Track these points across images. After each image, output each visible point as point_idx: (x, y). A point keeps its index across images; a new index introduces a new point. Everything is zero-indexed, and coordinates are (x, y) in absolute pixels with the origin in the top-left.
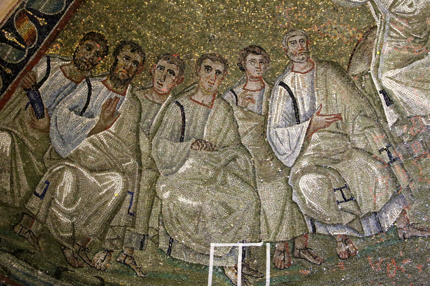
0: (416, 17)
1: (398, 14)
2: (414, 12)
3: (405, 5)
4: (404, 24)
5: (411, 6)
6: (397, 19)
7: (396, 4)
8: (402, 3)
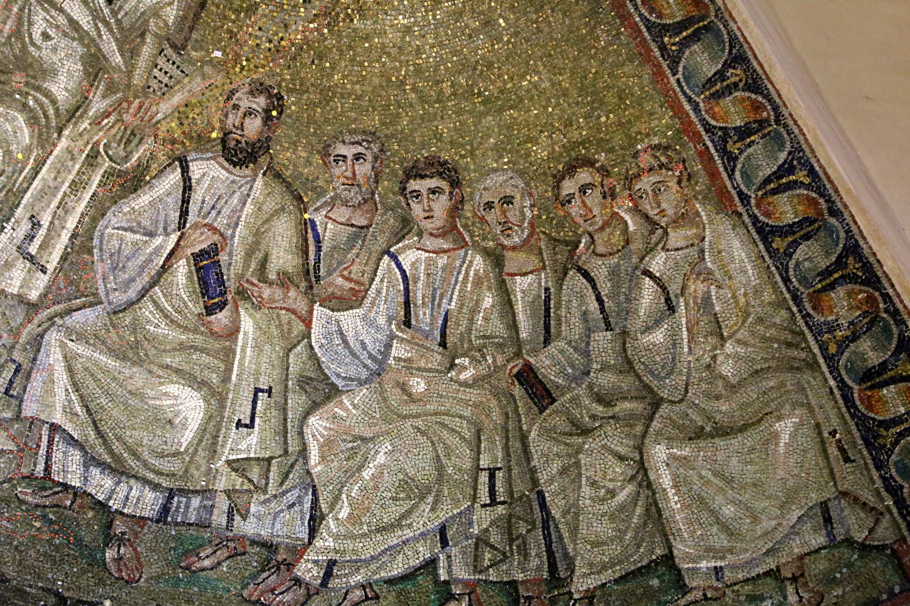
0: (24, 49)
1: (26, 11)
2: (34, 44)
3: (44, 25)
4: (7, 27)
5: (46, 36)
6: (15, 9)
7: (46, 5)
8: (48, 17)
